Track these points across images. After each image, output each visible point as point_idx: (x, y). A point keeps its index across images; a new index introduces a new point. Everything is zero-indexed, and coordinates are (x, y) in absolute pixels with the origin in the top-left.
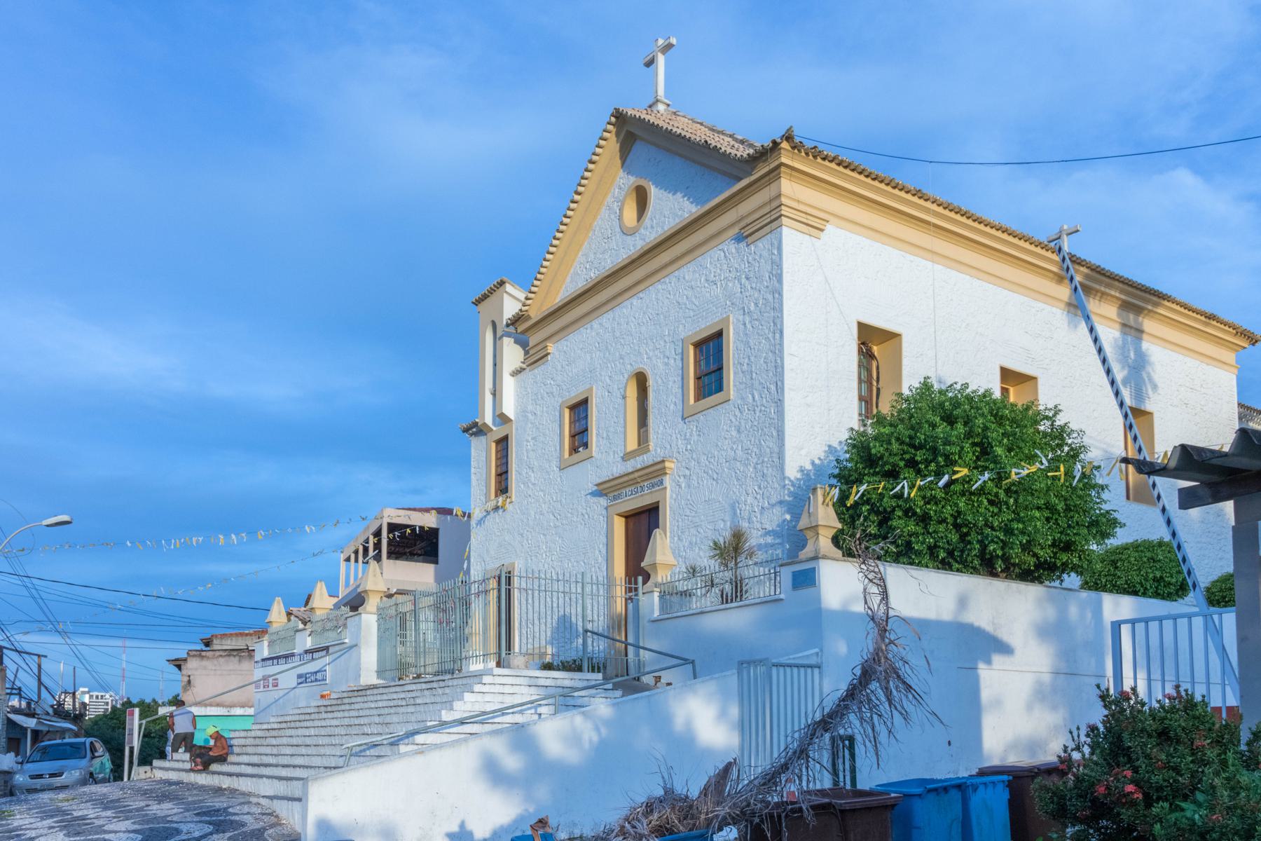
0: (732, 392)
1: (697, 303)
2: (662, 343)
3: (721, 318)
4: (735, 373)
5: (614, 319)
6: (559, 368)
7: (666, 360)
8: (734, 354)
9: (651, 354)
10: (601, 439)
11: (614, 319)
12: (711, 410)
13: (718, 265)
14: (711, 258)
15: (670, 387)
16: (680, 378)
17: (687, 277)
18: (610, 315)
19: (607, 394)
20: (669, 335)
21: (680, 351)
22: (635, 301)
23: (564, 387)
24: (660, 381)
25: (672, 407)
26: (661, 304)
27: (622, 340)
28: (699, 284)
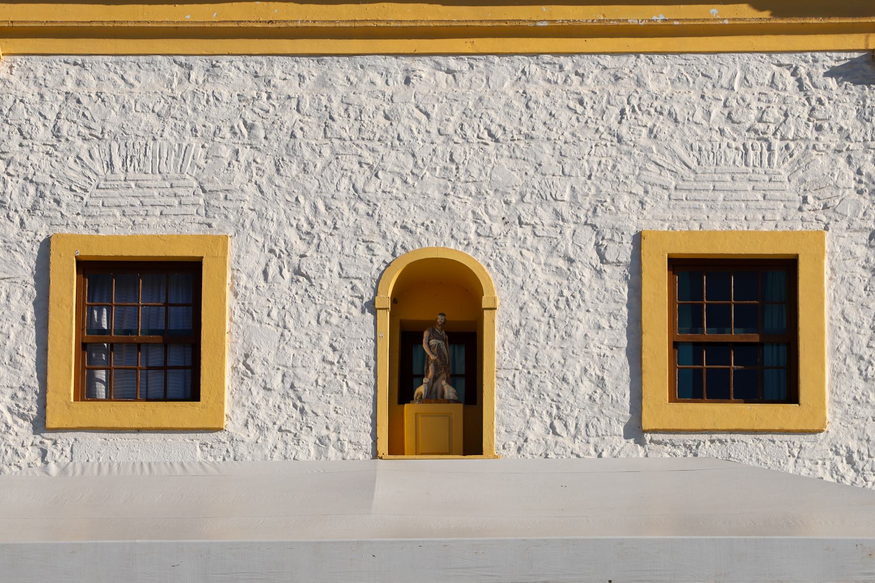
0: (828, 416)
1: (694, 164)
2: (546, 216)
3: (783, 227)
4: (837, 374)
5: (324, 82)
6: (43, 134)
7: (562, 264)
8: (835, 332)
9: (497, 228)
10: (258, 395)
11: (324, 82)
12: (749, 438)
13: (775, 99)
14: (745, 69)
15: (578, 335)
16: (621, 325)
17: (652, 87)
18: (309, 67)
19: (287, 274)
20: (574, 202)
21: (626, 256)
22: (423, 68)
23: (66, 197)
24: (534, 309)
25: (586, 387)
26: (544, 115)
27: (368, 158)
28: (699, 116)
